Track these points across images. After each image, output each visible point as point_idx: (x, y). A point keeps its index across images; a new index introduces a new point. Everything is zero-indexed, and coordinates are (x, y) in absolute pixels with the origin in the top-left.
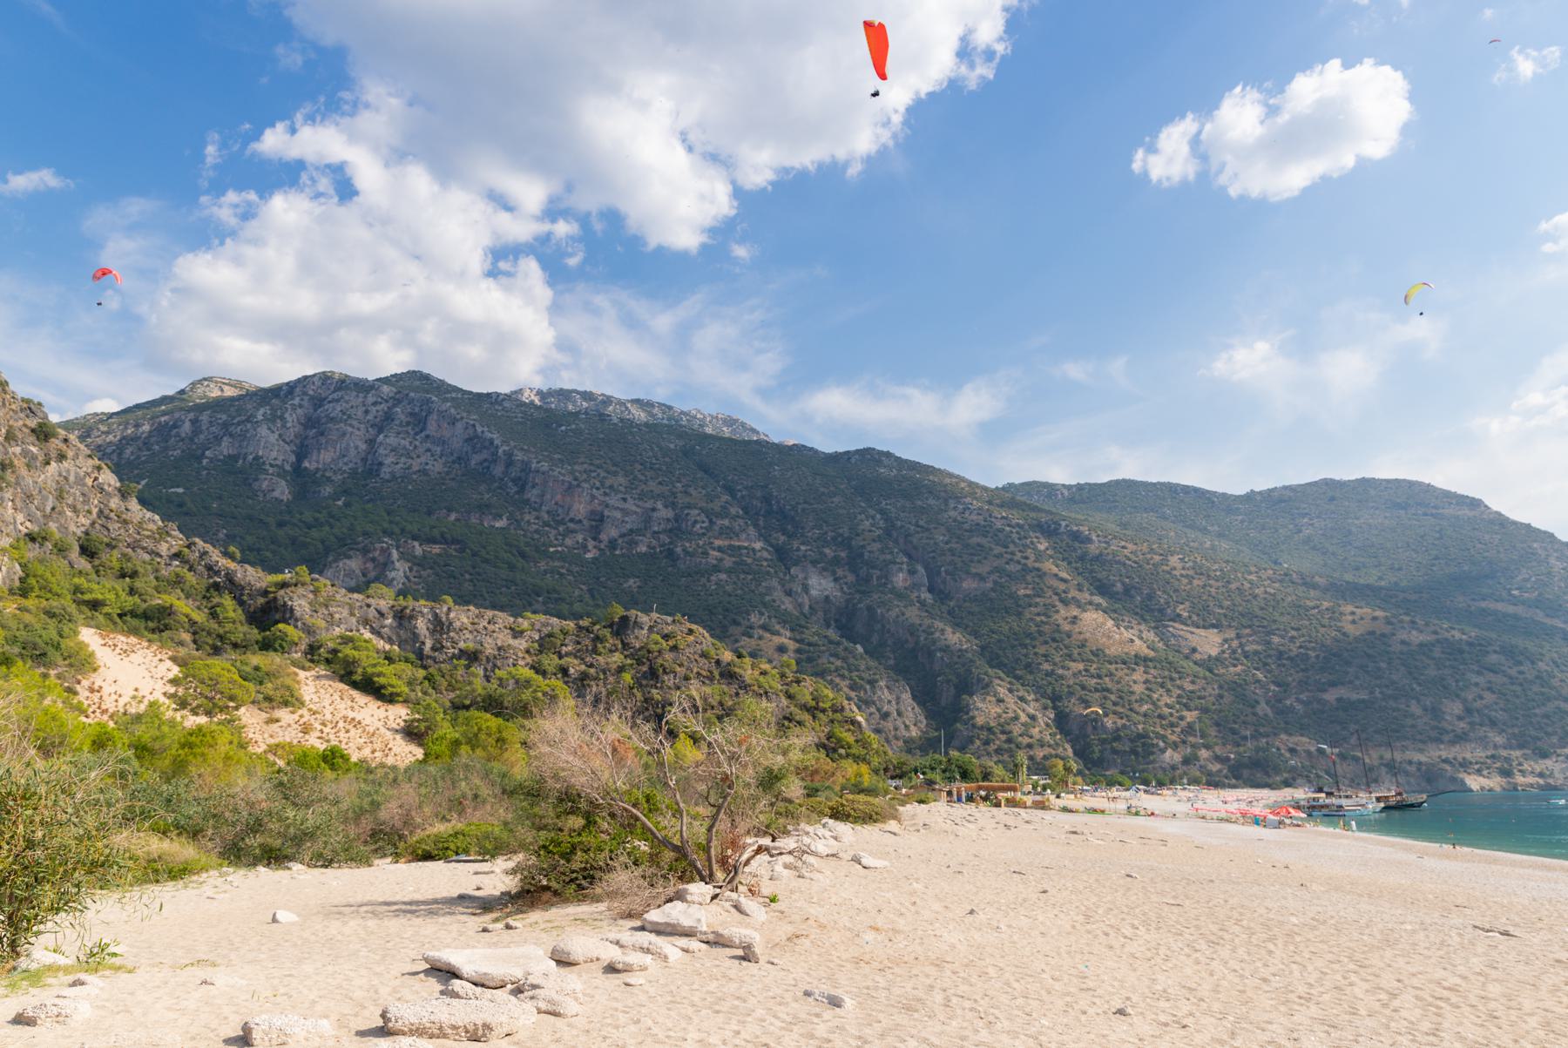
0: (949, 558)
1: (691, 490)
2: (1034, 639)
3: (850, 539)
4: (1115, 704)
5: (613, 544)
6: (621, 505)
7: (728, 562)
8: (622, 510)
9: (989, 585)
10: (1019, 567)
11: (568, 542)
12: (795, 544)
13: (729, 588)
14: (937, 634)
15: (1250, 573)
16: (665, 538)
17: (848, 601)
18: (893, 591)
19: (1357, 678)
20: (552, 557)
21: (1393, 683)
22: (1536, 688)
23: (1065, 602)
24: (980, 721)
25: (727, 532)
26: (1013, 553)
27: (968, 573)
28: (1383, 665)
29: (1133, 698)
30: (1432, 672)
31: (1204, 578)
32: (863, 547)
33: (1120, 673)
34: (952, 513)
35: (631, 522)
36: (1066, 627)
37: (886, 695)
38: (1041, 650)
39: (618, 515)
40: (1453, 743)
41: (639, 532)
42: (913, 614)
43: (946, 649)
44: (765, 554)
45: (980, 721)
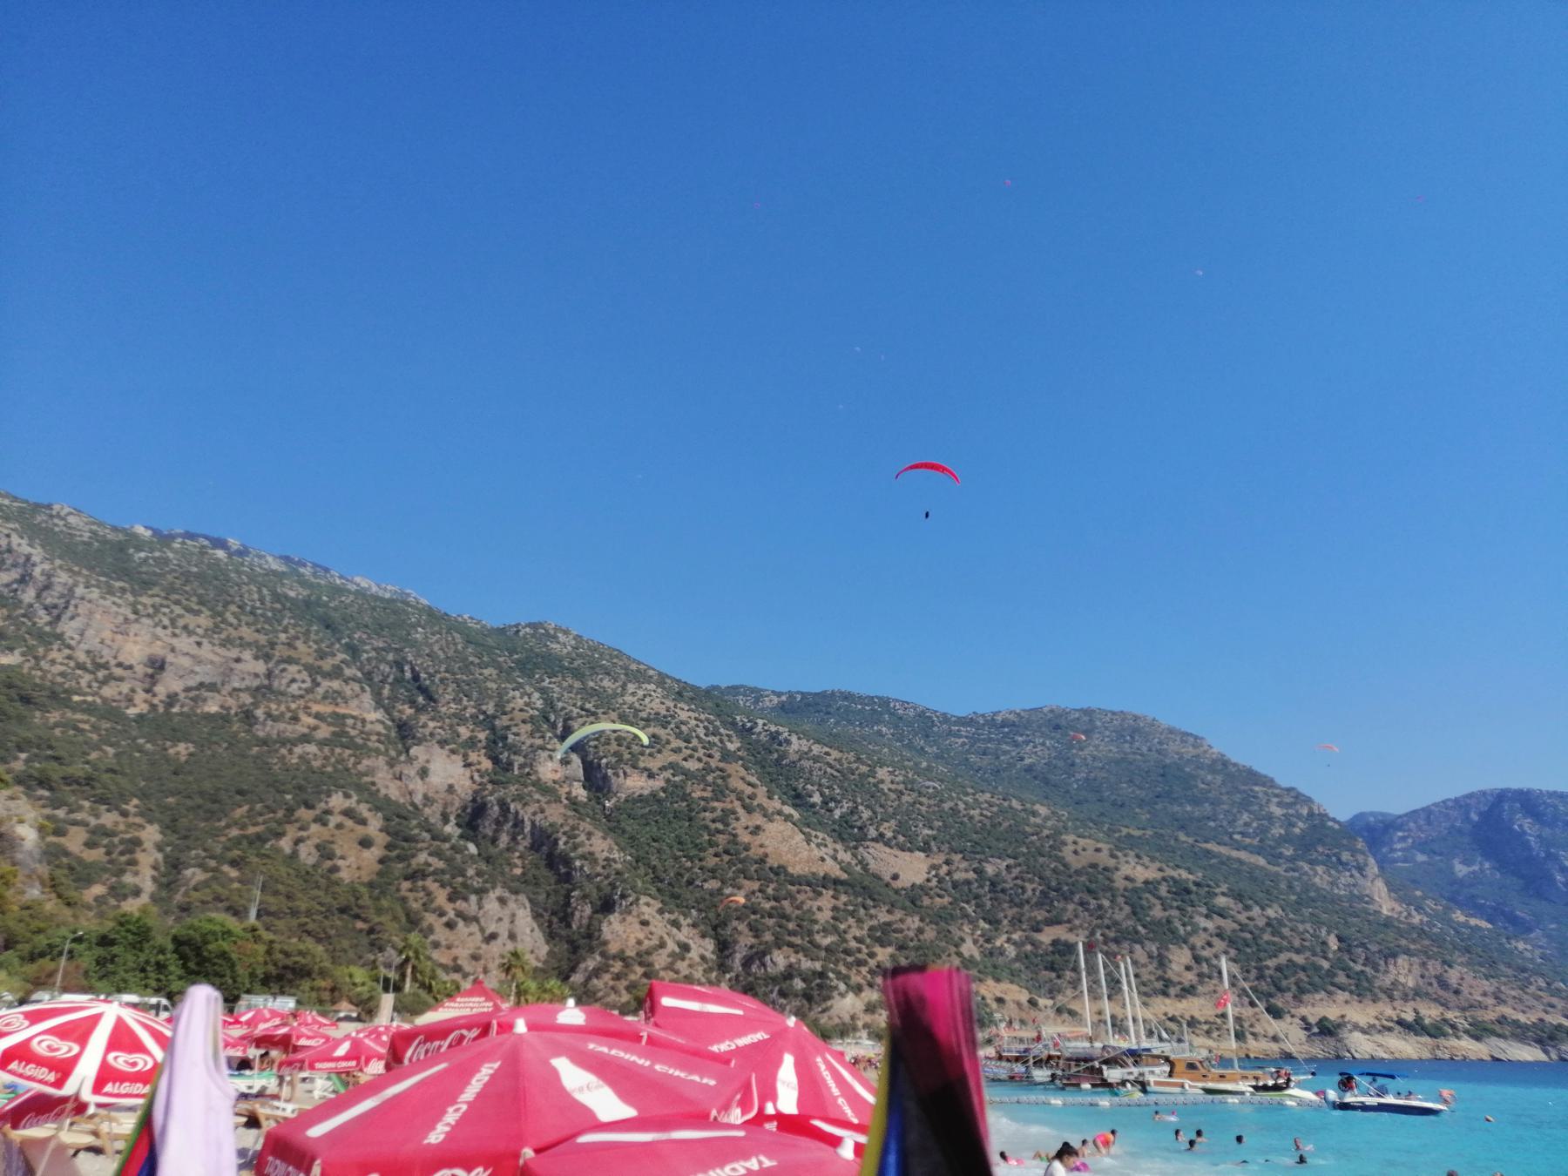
0: (614, 747)
1: (299, 644)
2: (702, 850)
3: (494, 717)
4: (791, 933)
5: (172, 699)
6: (194, 650)
7: (324, 732)
8: (193, 657)
9: (658, 783)
10: (701, 766)
11: (107, 691)
12: (423, 718)
13: (316, 764)
14: (583, 837)
15: (967, 794)
16: (247, 699)
17: (476, 792)
18: (538, 784)
19: (1076, 916)
20: (75, 708)
21: (1116, 923)
22: (1267, 937)
23: (749, 810)
24: (613, 948)
25: (333, 697)
26: (695, 749)
27: (634, 767)
28: (1106, 903)
29: (816, 927)
30: (1157, 913)
31: (915, 795)
32: (508, 728)
33: (800, 897)
34: (629, 699)
35: (205, 674)
36: (745, 838)
38: (711, 862)
39: (186, 662)
40: (1179, 997)
41: (212, 687)
42: (555, 814)
43: (590, 857)
44: (380, 728)
45: (613, 948)
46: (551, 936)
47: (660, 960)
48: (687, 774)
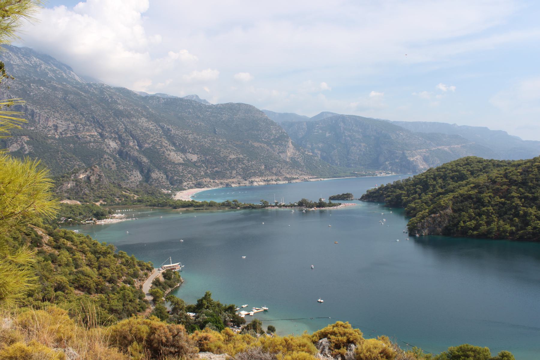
5: (61, 134)
18: (130, 147)
37: (134, 172)
38: (163, 162)
43: (144, 162)
46: (142, 175)
47: (160, 179)
48: (155, 142)
